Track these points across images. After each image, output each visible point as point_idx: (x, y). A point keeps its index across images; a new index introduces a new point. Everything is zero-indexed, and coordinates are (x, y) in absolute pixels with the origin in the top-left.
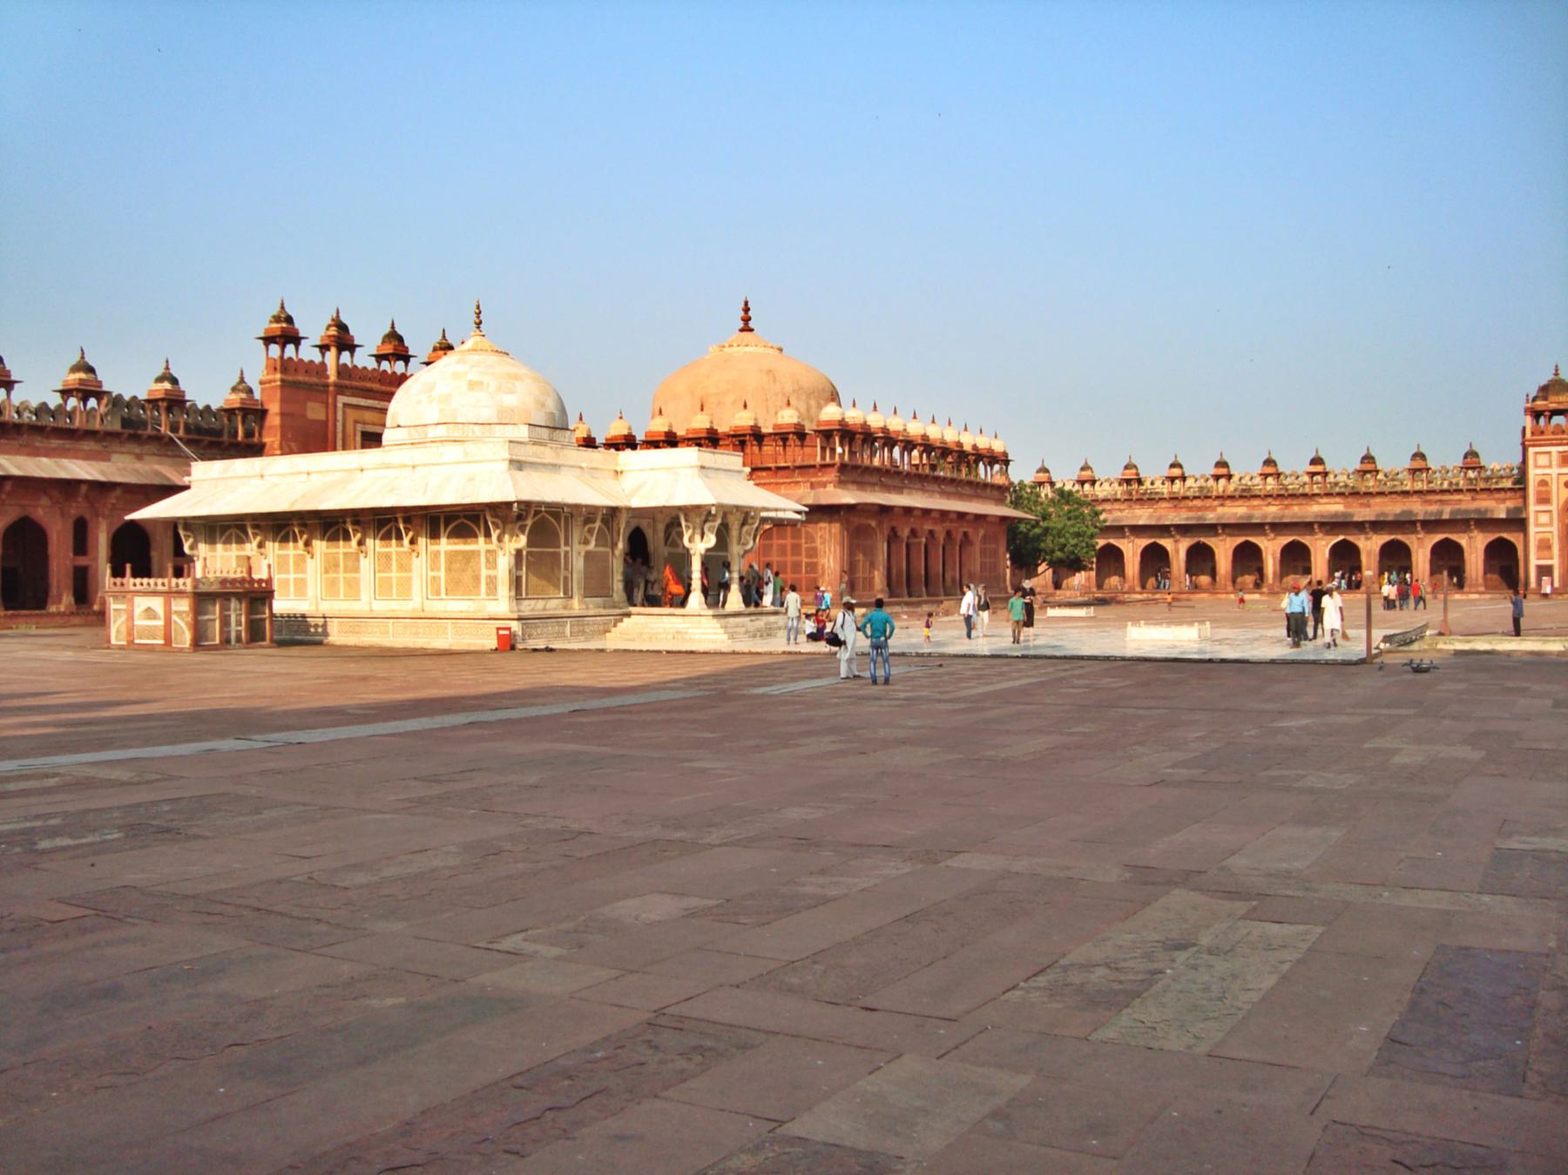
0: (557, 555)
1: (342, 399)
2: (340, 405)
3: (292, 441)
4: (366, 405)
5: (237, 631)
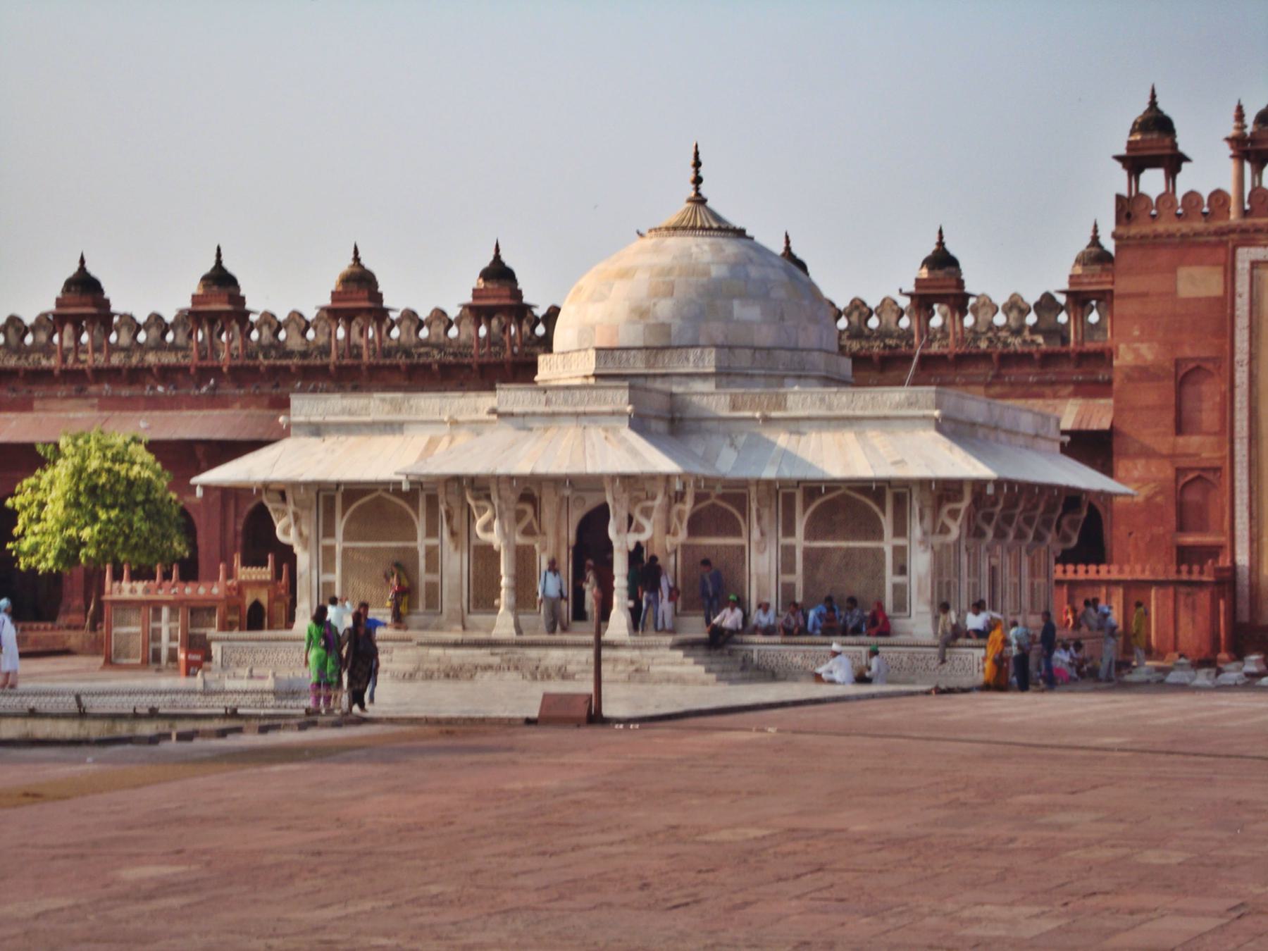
0: (414, 552)
1: (1245, 256)
3: (1142, 342)
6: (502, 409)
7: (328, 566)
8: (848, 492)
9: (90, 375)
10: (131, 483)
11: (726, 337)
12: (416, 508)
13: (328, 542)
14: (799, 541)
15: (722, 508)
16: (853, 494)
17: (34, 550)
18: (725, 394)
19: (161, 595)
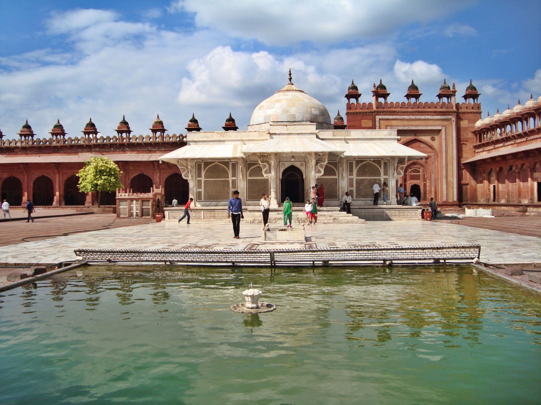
0: (228, 181)
1: (378, 117)
2: (377, 120)
4: (393, 118)
5: (136, 212)
6: (271, 132)
7: (199, 186)
8: (369, 162)
9: (93, 146)
10: (110, 169)
11: (311, 119)
12: (228, 168)
13: (199, 179)
14: (355, 177)
15: (329, 166)
16: (371, 162)
17: (84, 186)
18: (331, 131)
19: (133, 197)
